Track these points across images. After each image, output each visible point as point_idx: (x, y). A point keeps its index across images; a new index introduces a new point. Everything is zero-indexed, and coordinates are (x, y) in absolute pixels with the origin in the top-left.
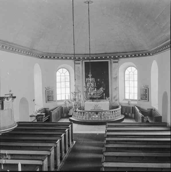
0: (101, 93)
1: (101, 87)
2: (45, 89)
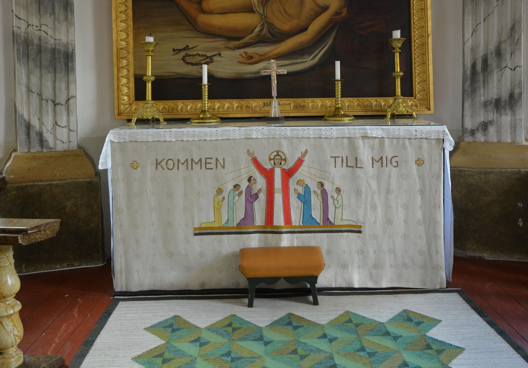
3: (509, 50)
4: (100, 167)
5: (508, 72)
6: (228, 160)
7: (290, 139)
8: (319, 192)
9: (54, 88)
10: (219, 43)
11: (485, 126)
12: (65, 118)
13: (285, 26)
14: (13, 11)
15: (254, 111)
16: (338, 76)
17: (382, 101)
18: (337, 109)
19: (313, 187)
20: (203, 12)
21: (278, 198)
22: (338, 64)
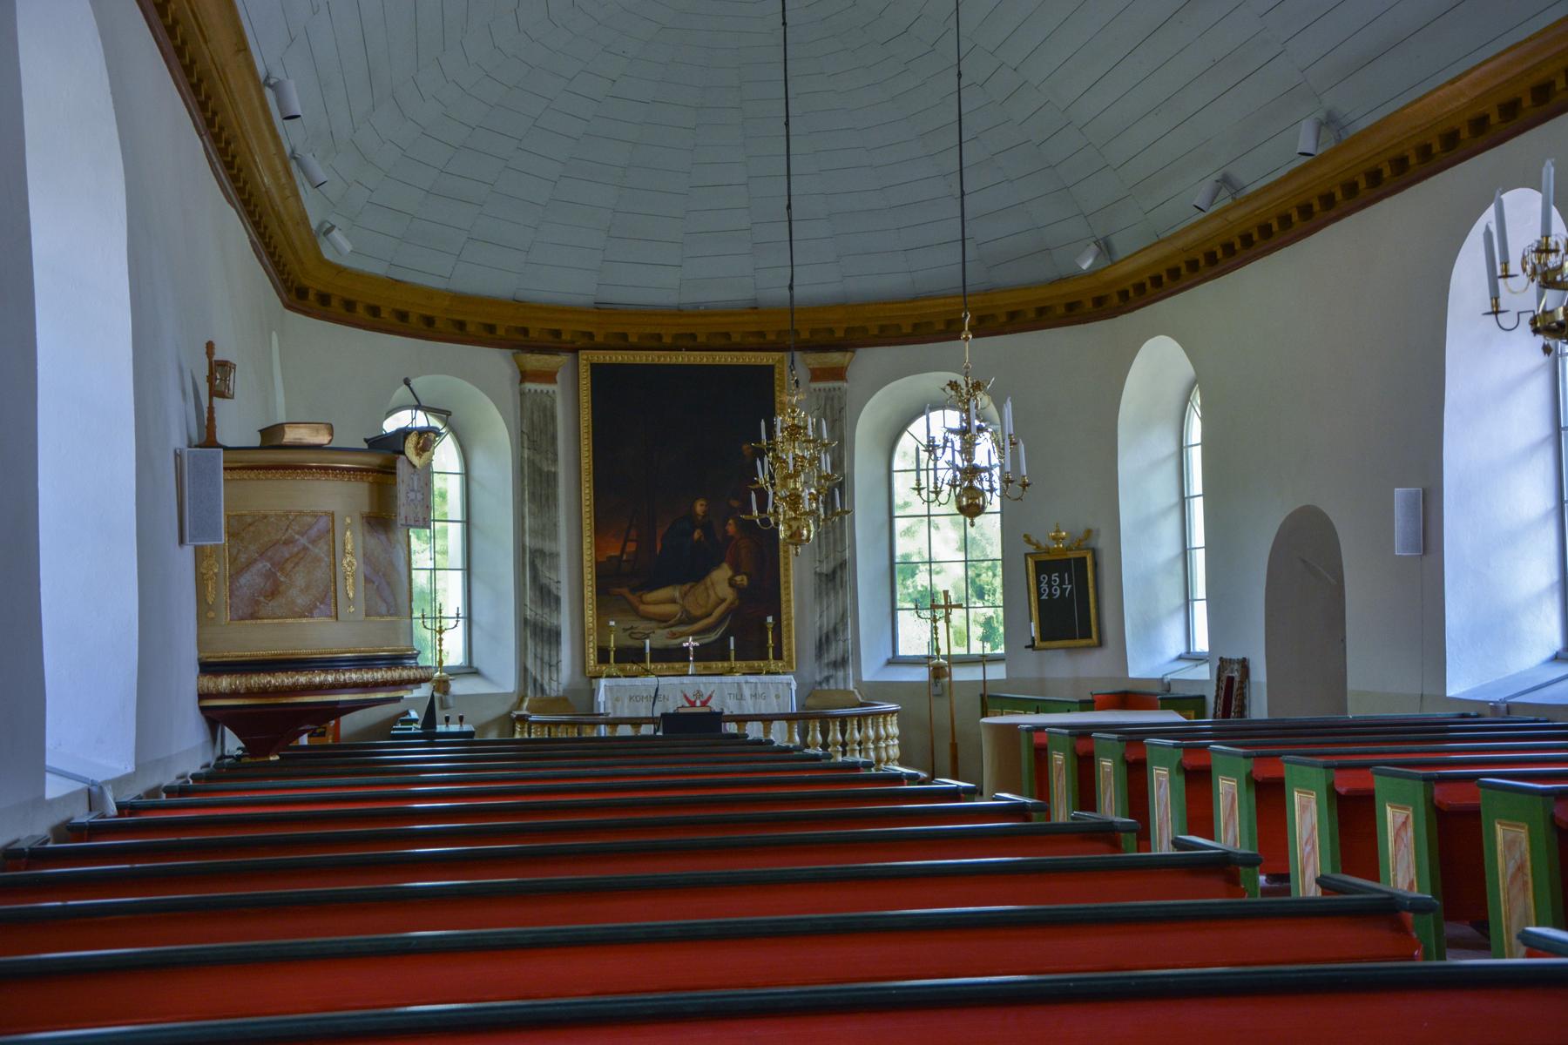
1: (717, 565)
3: (841, 628)
5: (841, 643)
6: (670, 696)
7: (705, 684)
10: (653, 624)
11: (827, 679)
12: (556, 675)
13: (698, 612)
14: (526, 605)
15: (678, 671)
16: (732, 647)
18: (732, 668)
20: (644, 603)
22: (732, 638)
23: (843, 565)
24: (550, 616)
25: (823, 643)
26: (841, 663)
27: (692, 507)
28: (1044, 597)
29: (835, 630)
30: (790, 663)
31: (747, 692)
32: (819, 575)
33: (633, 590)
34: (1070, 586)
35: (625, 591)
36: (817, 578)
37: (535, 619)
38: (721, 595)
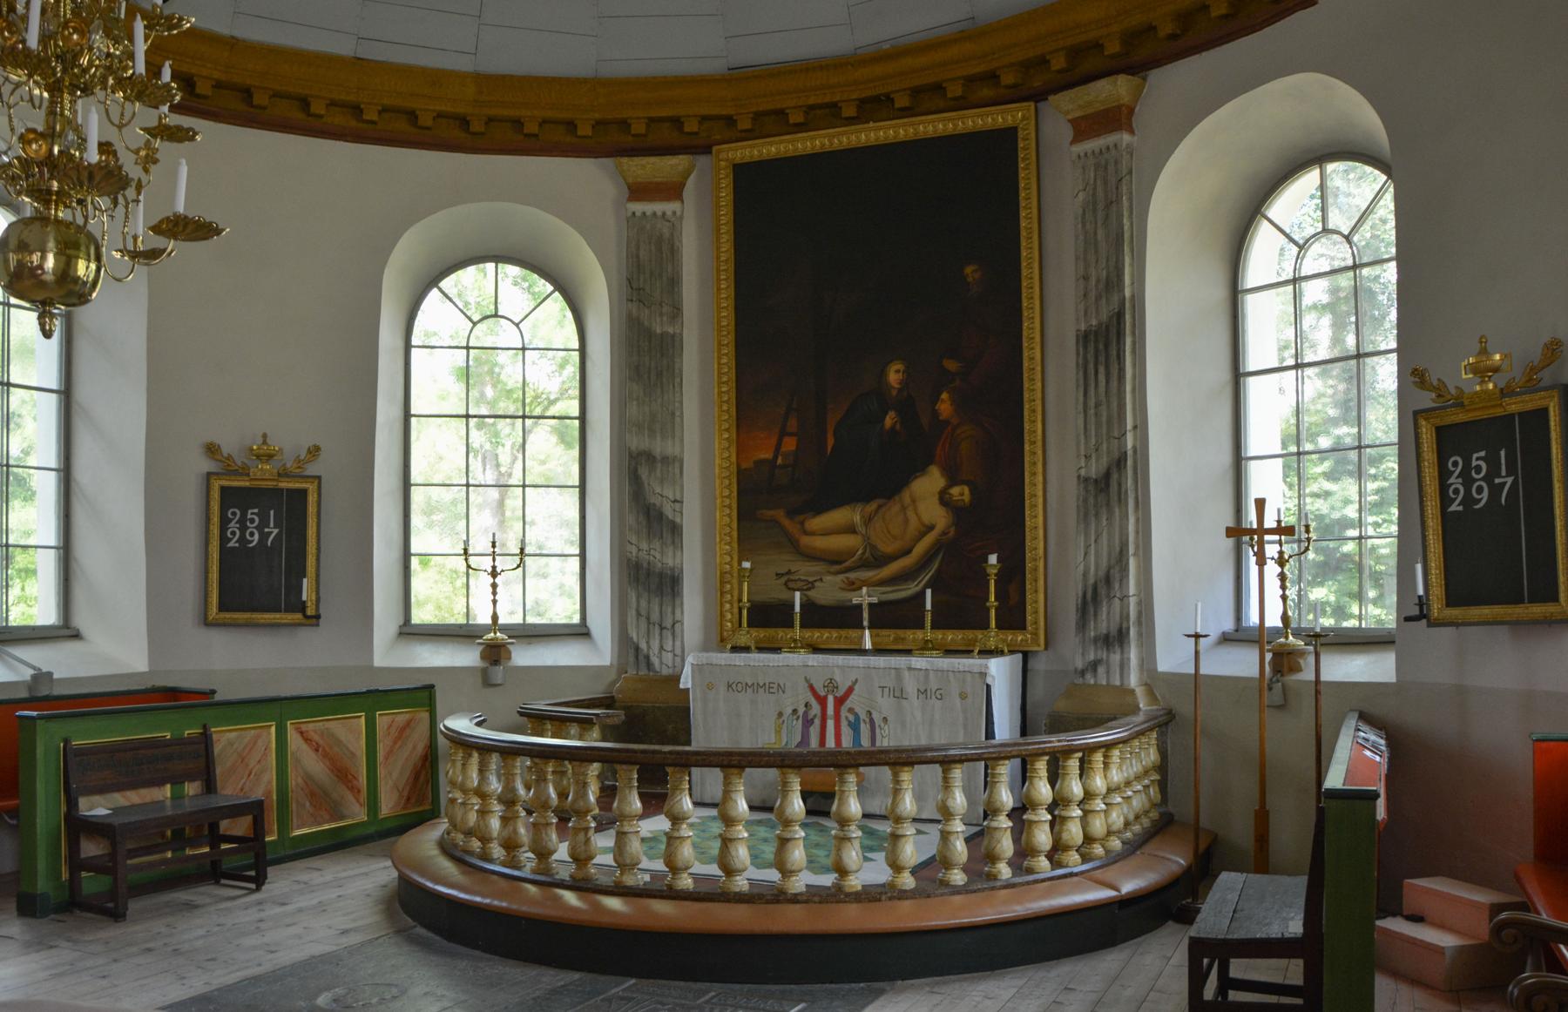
0: (920, 548)
1: (919, 469)
2: (207, 465)
4: (681, 686)
7: (842, 668)
8: (868, 720)
9: (661, 612)
12: (670, 643)
13: (888, 548)
16: (929, 606)
17: (970, 634)
19: (863, 716)
21: (830, 724)
22: (929, 592)
23: (1120, 462)
24: (662, 553)
25: (1090, 602)
26: (1117, 639)
27: (882, 374)
28: (1454, 507)
29: (1108, 580)
30: (1035, 634)
31: (911, 687)
32: (1084, 481)
33: (792, 513)
34: (1510, 480)
35: (779, 514)
36: (1082, 485)
37: (637, 557)
38: (926, 519)
